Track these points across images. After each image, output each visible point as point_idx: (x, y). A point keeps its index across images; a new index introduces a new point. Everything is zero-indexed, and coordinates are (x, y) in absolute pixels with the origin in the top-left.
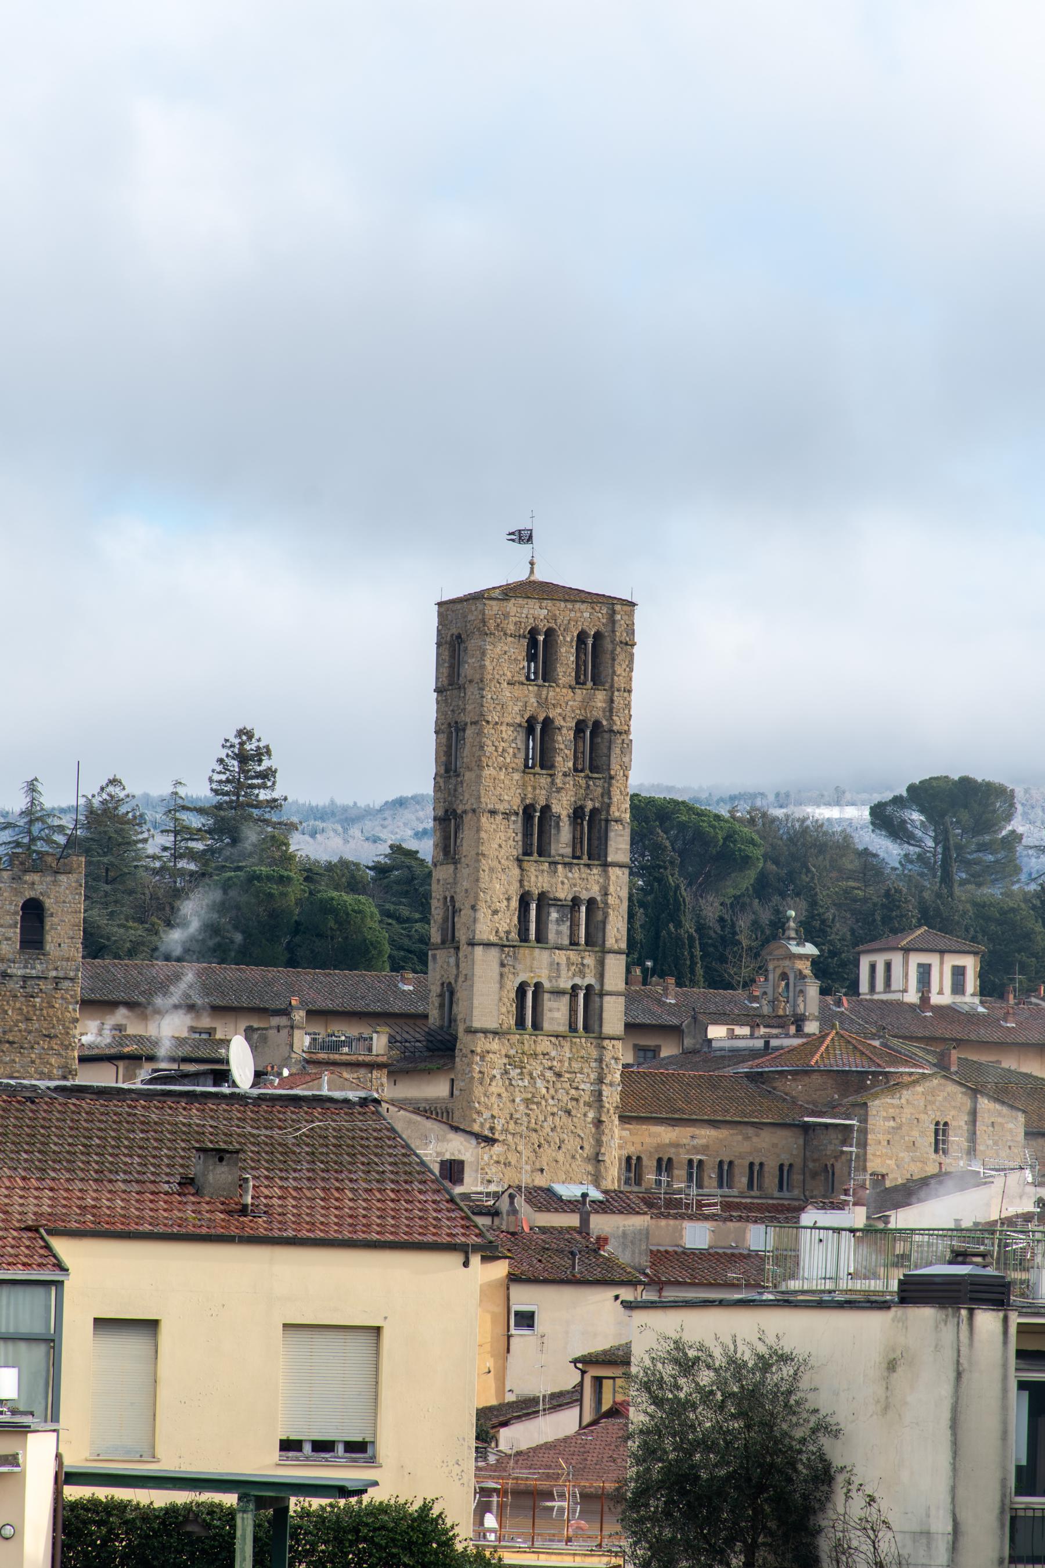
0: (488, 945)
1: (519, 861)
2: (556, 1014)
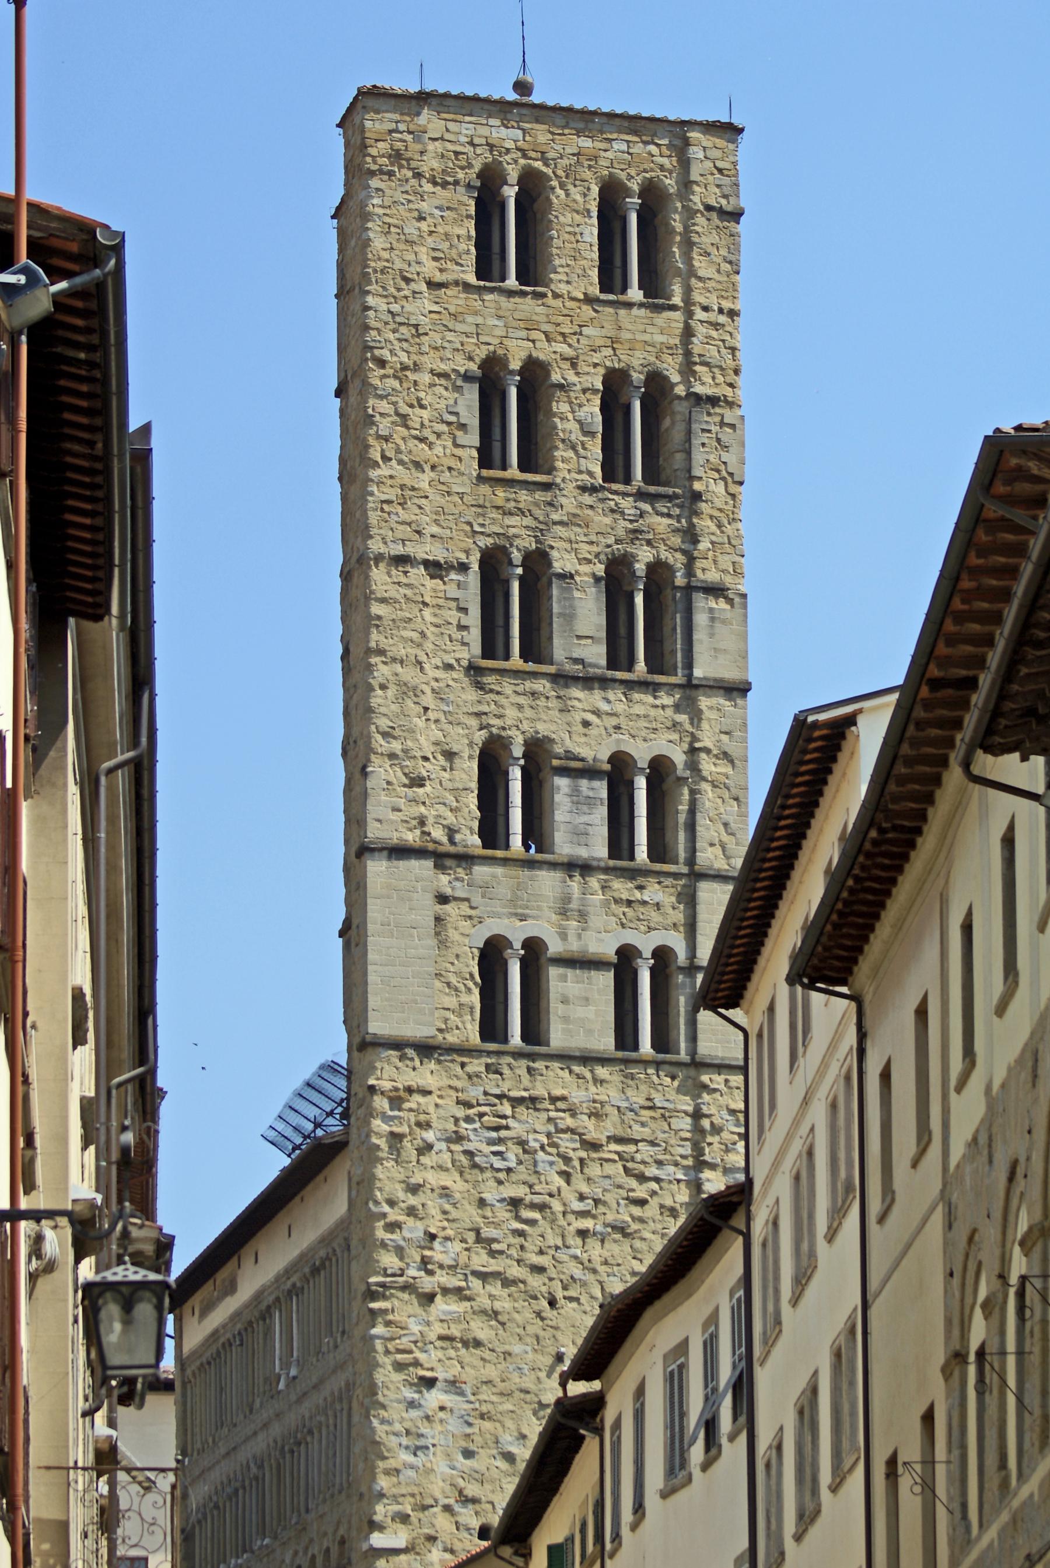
1: (473, 670)
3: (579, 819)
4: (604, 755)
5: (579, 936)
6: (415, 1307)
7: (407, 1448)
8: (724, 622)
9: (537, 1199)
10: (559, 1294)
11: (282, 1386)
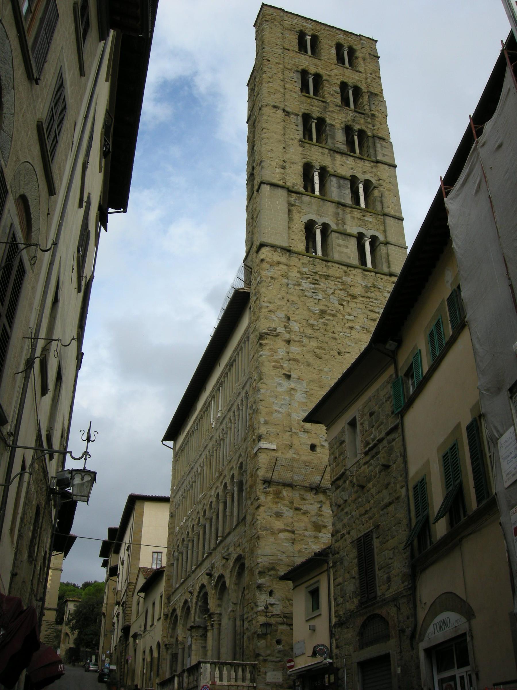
3: (340, 192)
5: (343, 227)
7: (277, 404)
9: (332, 312)
11: (213, 426)
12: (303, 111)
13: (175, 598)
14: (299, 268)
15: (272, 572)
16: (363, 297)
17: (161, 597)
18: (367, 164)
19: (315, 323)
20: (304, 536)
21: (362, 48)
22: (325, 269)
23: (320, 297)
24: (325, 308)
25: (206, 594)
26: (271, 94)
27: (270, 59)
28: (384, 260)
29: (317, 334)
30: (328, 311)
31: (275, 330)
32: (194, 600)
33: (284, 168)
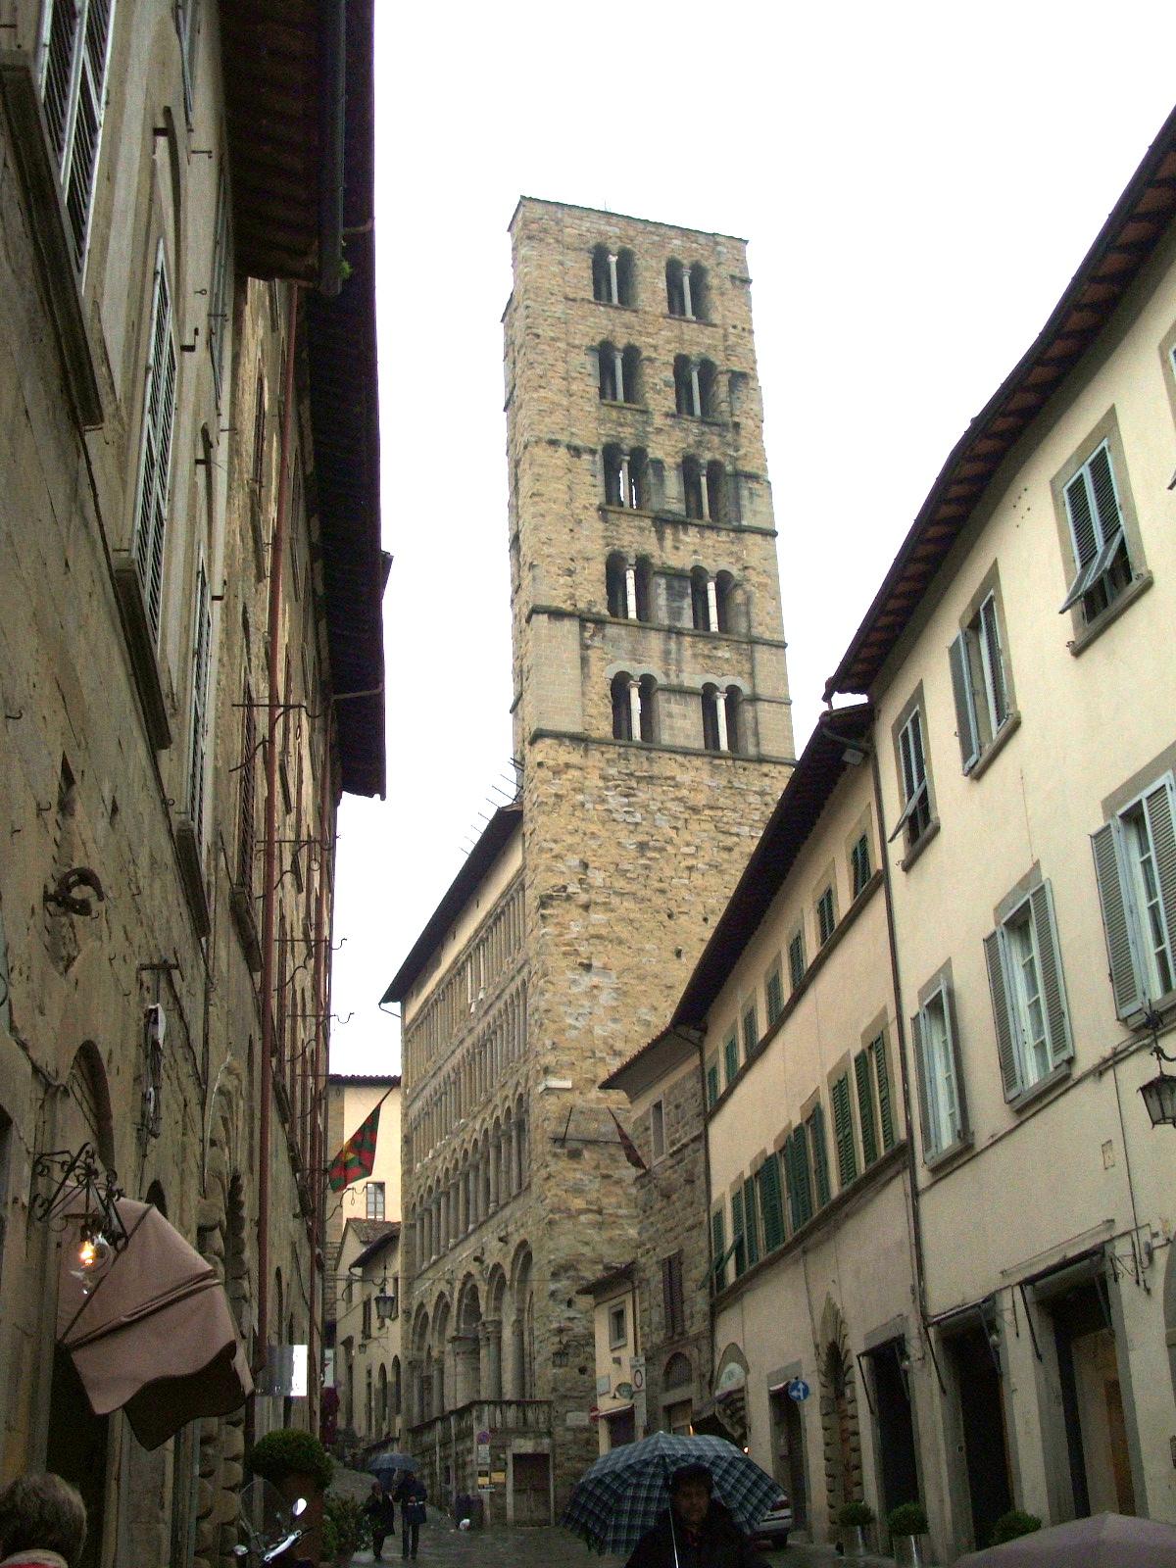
0: (556, 614)
1: (600, 509)
2: (682, 723)
4: (689, 567)
5: (678, 676)
6: (576, 912)
7: (571, 1014)
8: (758, 496)
9: (658, 844)
10: (675, 910)
11: (473, 1010)
12: (604, 439)
13: (422, 1287)
14: (602, 769)
15: (571, 1273)
16: (711, 808)
17: (396, 1280)
18: (723, 537)
19: (630, 867)
20: (617, 1216)
21: (719, 264)
22: (646, 765)
23: (638, 818)
24: (646, 838)
25: (475, 1288)
26: (543, 413)
27: (540, 332)
28: (749, 733)
29: (634, 887)
30: (651, 843)
31: (565, 888)
32: (456, 1295)
33: (570, 573)
